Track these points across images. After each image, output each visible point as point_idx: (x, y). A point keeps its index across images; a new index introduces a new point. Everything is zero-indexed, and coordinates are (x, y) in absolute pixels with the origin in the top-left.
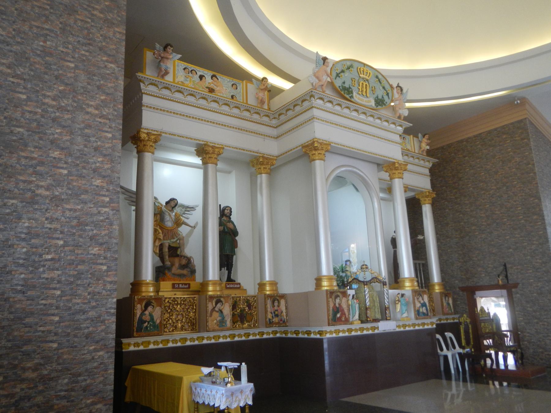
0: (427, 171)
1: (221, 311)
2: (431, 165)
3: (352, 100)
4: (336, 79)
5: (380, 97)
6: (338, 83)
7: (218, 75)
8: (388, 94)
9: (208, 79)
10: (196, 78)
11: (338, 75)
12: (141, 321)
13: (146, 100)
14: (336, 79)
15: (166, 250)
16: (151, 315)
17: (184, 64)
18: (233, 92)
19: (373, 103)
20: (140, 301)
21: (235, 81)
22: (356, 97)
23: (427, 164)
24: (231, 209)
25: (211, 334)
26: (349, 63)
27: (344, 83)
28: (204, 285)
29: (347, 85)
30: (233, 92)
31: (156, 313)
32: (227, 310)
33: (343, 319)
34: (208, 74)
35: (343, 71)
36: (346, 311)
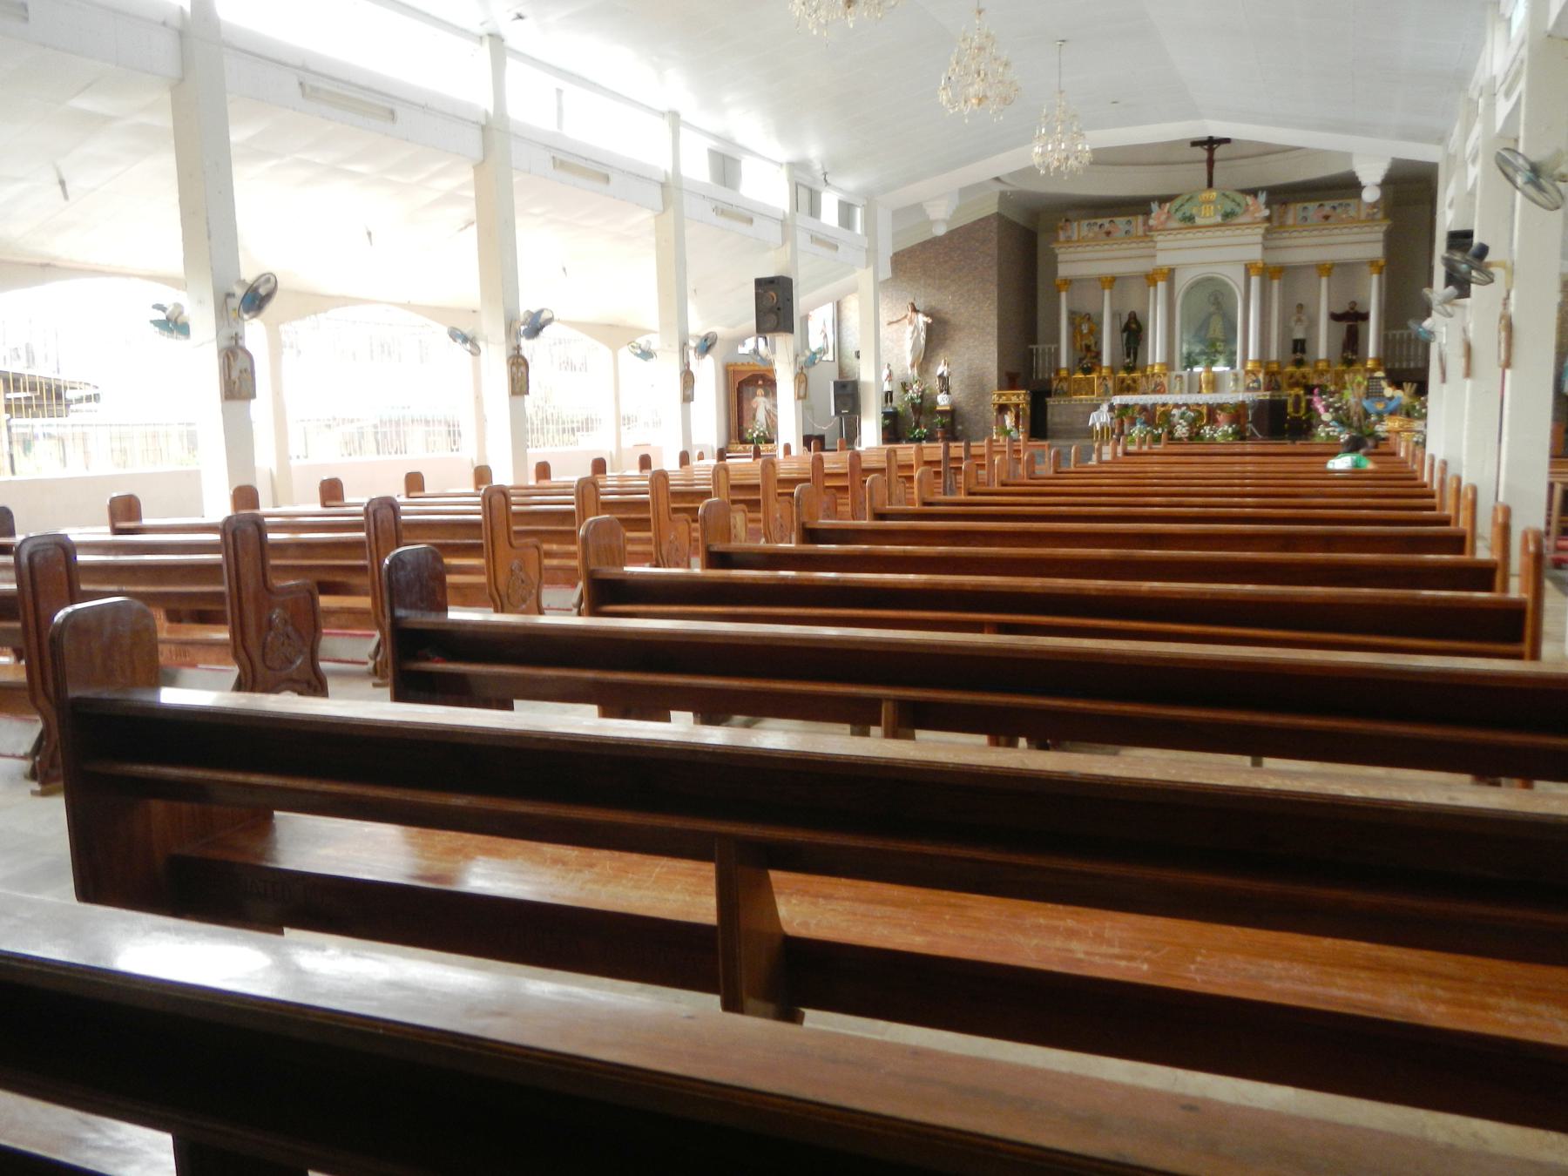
0: (1381, 236)
1: (1106, 385)
2: (1384, 228)
3: (1195, 224)
4: (1175, 213)
5: (1229, 210)
6: (1179, 215)
7: (1114, 219)
8: (1239, 205)
9: (1107, 225)
10: (1096, 229)
11: (1177, 210)
12: (1056, 390)
13: (1060, 258)
14: (1175, 213)
15: (1084, 347)
16: (1062, 387)
17: (1086, 222)
18: (1127, 228)
19: (1219, 219)
20: (1056, 380)
21: (1130, 218)
22: (1199, 221)
23: (1377, 228)
24: (1135, 315)
25: (1099, 398)
26: (1187, 197)
27: (1184, 214)
28: (1101, 370)
29: (1188, 214)
30: (1127, 228)
31: (1065, 385)
32: (1110, 384)
33: (1162, 390)
34: (1105, 221)
35: (1182, 205)
36: (1166, 386)
